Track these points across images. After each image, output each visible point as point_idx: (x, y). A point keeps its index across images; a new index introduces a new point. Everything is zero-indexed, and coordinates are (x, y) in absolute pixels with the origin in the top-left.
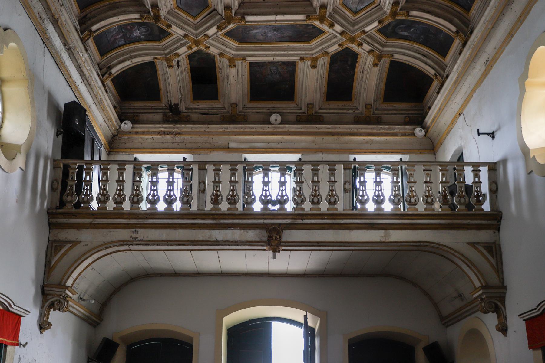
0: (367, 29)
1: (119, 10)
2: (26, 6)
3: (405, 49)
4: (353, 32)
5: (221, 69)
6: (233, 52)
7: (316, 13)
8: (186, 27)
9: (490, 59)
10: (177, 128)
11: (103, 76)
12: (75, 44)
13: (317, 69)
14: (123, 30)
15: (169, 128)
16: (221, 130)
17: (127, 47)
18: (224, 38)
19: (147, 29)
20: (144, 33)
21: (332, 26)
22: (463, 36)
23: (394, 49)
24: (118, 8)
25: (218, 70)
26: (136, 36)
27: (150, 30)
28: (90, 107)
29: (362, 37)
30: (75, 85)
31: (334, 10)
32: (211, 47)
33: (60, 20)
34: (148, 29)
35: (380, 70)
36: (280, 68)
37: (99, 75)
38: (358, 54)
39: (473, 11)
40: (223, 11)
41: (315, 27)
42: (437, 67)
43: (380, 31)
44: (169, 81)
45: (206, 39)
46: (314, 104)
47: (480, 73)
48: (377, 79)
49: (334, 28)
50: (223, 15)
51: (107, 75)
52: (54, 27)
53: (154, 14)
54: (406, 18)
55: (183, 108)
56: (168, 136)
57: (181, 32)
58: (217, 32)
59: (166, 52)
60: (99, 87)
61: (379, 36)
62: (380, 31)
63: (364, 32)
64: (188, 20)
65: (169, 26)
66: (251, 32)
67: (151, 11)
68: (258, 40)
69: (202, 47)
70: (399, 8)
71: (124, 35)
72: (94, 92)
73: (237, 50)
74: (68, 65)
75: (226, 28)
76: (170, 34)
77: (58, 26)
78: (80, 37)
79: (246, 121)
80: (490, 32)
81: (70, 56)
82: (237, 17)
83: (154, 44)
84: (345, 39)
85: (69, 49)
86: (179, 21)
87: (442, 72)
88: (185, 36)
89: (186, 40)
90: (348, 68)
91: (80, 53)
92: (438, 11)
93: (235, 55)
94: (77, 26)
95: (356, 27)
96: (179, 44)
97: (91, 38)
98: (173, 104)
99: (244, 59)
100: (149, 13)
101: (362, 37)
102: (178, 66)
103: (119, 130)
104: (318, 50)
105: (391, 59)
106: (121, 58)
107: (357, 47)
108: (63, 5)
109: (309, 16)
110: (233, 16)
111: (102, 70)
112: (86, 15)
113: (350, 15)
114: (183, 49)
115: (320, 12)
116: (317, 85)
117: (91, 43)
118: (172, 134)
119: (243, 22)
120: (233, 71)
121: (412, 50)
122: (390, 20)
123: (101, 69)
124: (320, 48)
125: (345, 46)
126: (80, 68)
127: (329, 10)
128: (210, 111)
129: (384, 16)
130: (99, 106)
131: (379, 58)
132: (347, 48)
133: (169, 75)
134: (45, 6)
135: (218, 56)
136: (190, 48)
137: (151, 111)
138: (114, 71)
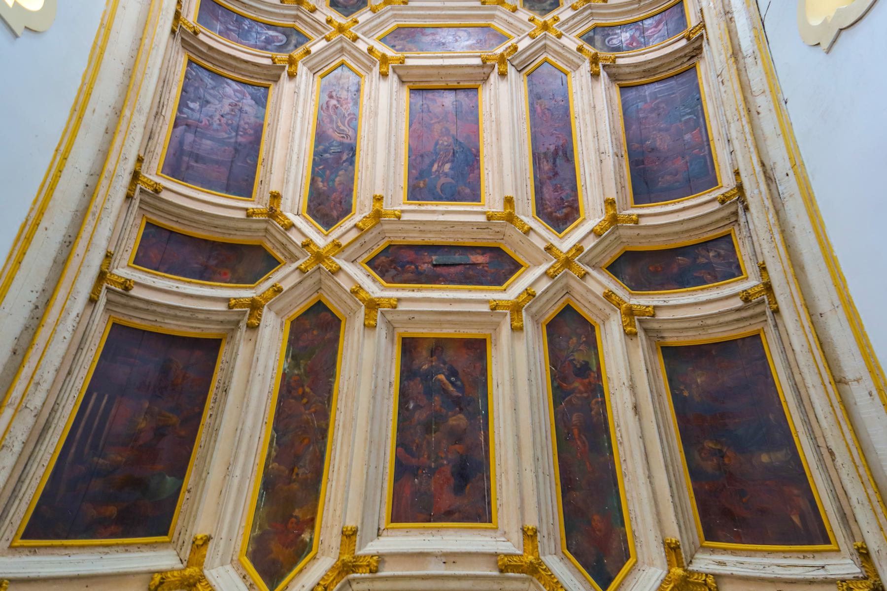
0: (324, 43)
1: (643, 68)
2: (772, 75)
3: (267, 11)
7: (392, 67)
8: (557, 48)
14: (643, 40)
17: (641, 15)
18: (510, 33)
20: (615, 36)
21: (371, 50)
24: (644, 71)
26: (626, 32)
29: (328, 33)
31: (371, 70)
34: (608, 42)
40: (509, 71)
41: (393, 47)
43: (307, 39)
53: (597, 64)
57: (564, 41)
61: (307, 31)
62: (307, 39)
63: (328, 39)
65: (580, 49)
66: (474, 42)
68: (465, 31)
70: (287, 68)
76: (580, 37)
83: (604, 22)
84: (351, 29)
86: (566, 56)
89: (560, 30)
92: (234, 63)
94: (707, 45)
95: (339, 46)
100: (604, 66)
101: (328, 33)
107: (333, 18)
115: (388, 69)
122: (297, 53)
124: (382, 18)
125: (350, 19)
127: (376, 70)
132: (347, 16)
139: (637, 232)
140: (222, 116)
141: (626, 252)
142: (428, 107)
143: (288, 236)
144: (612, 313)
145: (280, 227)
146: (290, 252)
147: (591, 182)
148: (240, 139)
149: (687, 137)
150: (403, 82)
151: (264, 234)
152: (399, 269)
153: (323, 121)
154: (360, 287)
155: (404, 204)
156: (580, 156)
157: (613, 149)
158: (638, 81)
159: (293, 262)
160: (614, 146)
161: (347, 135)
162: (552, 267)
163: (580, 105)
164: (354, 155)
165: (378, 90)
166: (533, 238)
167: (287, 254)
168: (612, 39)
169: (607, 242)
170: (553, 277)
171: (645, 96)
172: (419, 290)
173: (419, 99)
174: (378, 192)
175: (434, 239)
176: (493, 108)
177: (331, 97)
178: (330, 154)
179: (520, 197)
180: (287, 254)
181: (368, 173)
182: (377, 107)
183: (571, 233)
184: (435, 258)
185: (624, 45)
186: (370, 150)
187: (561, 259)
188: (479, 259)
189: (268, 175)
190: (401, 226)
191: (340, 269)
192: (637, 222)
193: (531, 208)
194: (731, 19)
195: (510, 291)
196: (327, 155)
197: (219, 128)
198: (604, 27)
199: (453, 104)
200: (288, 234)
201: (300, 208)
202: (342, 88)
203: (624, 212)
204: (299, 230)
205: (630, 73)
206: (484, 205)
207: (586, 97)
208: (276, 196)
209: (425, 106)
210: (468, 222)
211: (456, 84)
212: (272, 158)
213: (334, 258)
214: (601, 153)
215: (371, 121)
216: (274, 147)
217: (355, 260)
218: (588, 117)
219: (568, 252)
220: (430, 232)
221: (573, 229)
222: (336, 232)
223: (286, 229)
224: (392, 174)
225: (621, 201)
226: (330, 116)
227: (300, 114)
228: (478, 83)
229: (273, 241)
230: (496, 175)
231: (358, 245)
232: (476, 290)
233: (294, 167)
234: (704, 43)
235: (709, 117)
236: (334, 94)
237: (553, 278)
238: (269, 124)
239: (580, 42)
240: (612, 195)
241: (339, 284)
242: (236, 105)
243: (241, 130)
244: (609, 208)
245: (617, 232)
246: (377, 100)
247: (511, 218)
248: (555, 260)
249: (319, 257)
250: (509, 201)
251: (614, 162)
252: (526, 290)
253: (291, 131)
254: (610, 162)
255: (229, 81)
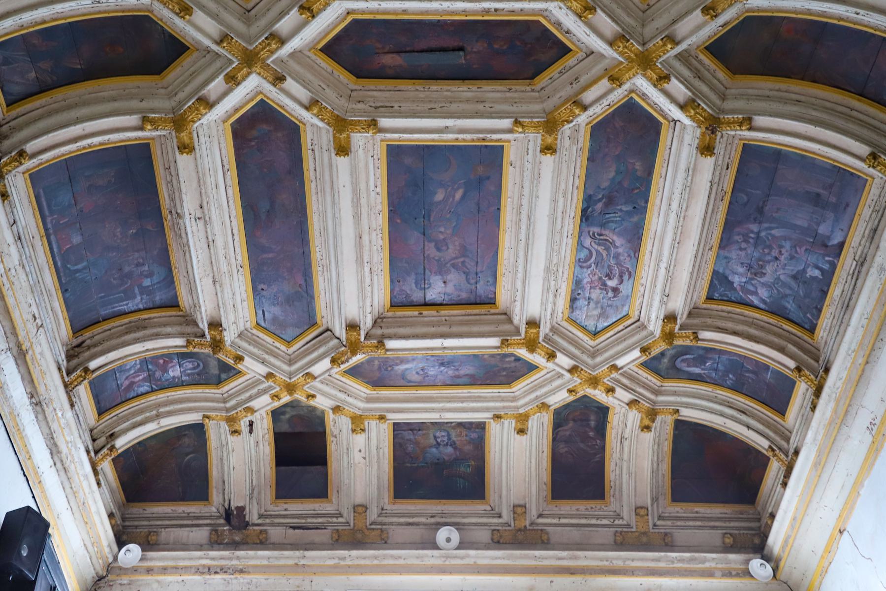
0: (620, 363)
4: (594, 367)
5: (335, 437)
6: (362, 405)
7: (520, 335)
8: (272, 360)
9: (877, 422)
10: (238, 558)
11: (96, 452)
12: (53, 394)
13: (528, 437)
14: (150, 367)
15: (221, 559)
16: (331, 562)
18: (343, 379)
19: (196, 364)
20: (189, 372)
21: (551, 356)
22: (812, 377)
23: (679, 399)
24: (145, 328)
25: (329, 438)
26: (174, 377)
27: (201, 365)
28: (60, 516)
29: (612, 376)
30: (36, 473)
31: (553, 329)
32: (318, 396)
33: (30, 352)
34: (198, 365)
35: (657, 439)
36: (453, 434)
37: (88, 452)
38: (607, 408)
39: (821, 333)
41: (518, 359)
42: (771, 434)
43: (645, 365)
44: (229, 461)
45: (309, 380)
46: (527, 506)
47: (864, 450)
48: (653, 455)
49: (557, 360)
50: (344, 338)
51: (105, 451)
52: (17, 364)
53: (214, 339)
54: (694, 343)
55: (253, 516)
56: (218, 577)
57: (263, 370)
58: (331, 368)
59: (228, 405)
60: (86, 477)
62: (645, 365)
63: (614, 368)
64: (276, 347)
65: (240, 359)
66: (396, 368)
67: (207, 333)
68: (410, 381)
69: (300, 396)
70: (677, 327)
71: (149, 375)
72: (73, 486)
73: (369, 400)
74: (29, 435)
75: (347, 361)
76: (239, 373)
77: (26, 362)
78: (64, 382)
79: (386, 542)
80: (863, 371)
81: (36, 417)
82: (369, 342)
84: (579, 381)
85: (37, 403)
86: (259, 349)
87: (784, 444)
88: (269, 376)
89: (270, 383)
90: (591, 434)
91: (58, 411)
93: (364, 410)
95: (599, 359)
96: (254, 391)
97: (86, 382)
98: (233, 508)
99: (382, 418)
100: (203, 336)
101: (612, 376)
102: (251, 432)
103: (114, 565)
104: (527, 399)
105: (676, 416)
106: (139, 418)
107: (604, 395)
108: (42, 326)
109: (507, 340)
110: (362, 339)
111: (97, 442)
112: (83, 342)
113: (585, 338)
114: (265, 399)
115: (526, 332)
116: (530, 468)
117: (83, 392)
118: (225, 572)
119: (380, 353)
120: (360, 439)
121: (715, 400)
122: (662, 346)
123: (94, 440)
124: (533, 396)
125: (581, 393)
126: (53, 438)
127: (544, 329)
128: (309, 520)
129: (650, 339)
130: (77, 515)
131: (652, 414)
132: (585, 396)
133: (230, 449)
134: (7, 329)
135: (331, 412)
136: (276, 397)
137: (185, 522)
138: (122, 443)
139: (144, 105)
140: (776, 259)
141: (159, 73)
142: (468, 280)
143: (690, 90)
145: (703, 105)
146: (689, 66)
147: (216, 176)
148: (755, 227)
149: (77, 239)
150: (505, 314)
151: (728, 91)
152: (518, 43)
153: (629, 256)
154: (580, 17)
155: (509, 141)
156: (233, 213)
157: (185, 224)
158: (152, 315)
159: (685, 50)
160: (182, 228)
161: (593, 237)
162: (272, 52)
163: (236, 284)
164: (584, 211)
165: (542, 303)
166: (303, 94)
167: (694, 62)
168: (194, 368)
169: (188, 89)
170: (273, 36)
171: (141, 294)
172: (487, 11)
173: (482, 289)
174: (548, 159)
175: (461, 89)
176: (368, 281)
177: (615, 290)
178: (621, 210)
179: (326, 155)
180: (694, 62)
181: (563, 186)
182: (546, 280)
183: (244, 101)
184: (459, 59)
185: (176, 361)
186: (559, 219)
187: (259, 65)
188: (389, 60)
189: (717, 179)
190: (514, 109)
191: (611, 44)
192: (145, 119)
193: (307, 137)
194: (32, 397)
195: (340, 12)
196: (624, 208)
197: (783, 243)
198: (207, 383)
199: (430, 284)
200: (690, 94)
201: (671, 131)
202: (597, 303)
203: (163, 133)
204: (673, 99)
205: (165, 325)
206: (382, 140)
207: (228, 294)
208: (707, 149)
209: (472, 281)
210: (406, 117)
211: (425, 313)
212: (708, 204)
213: (621, 59)
214: (203, 218)
215: (555, 261)
216: (705, 219)
217: (588, 56)
218: (224, 268)
219: (249, 74)
220: (468, 101)
221: (241, 108)
222: (618, 96)
223: (694, 101)
224: (527, 185)
225: (170, 149)
226: (619, 264)
227: (663, 265)
228: (390, 314)
229: (715, 81)
230: (363, 186)
231: (583, 80)
232: (395, 12)
233: (677, 192)
234: (64, 364)
235: (49, 268)
236: (611, 294)
237: (271, 34)
238: (710, 249)
239: (240, 366)
240: (183, 161)
241: (614, 20)
242: (755, 275)
243: (751, 241)
244: (186, 140)
245: (174, 104)
246: (546, 289)
247: (340, 124)
248: (269, 62)
249: (645, 62)
250: (343, 150)
251: (182, 206)
252: (313, 17)
253: (677, 243)
254: (189, 204)
255: (762, 306)
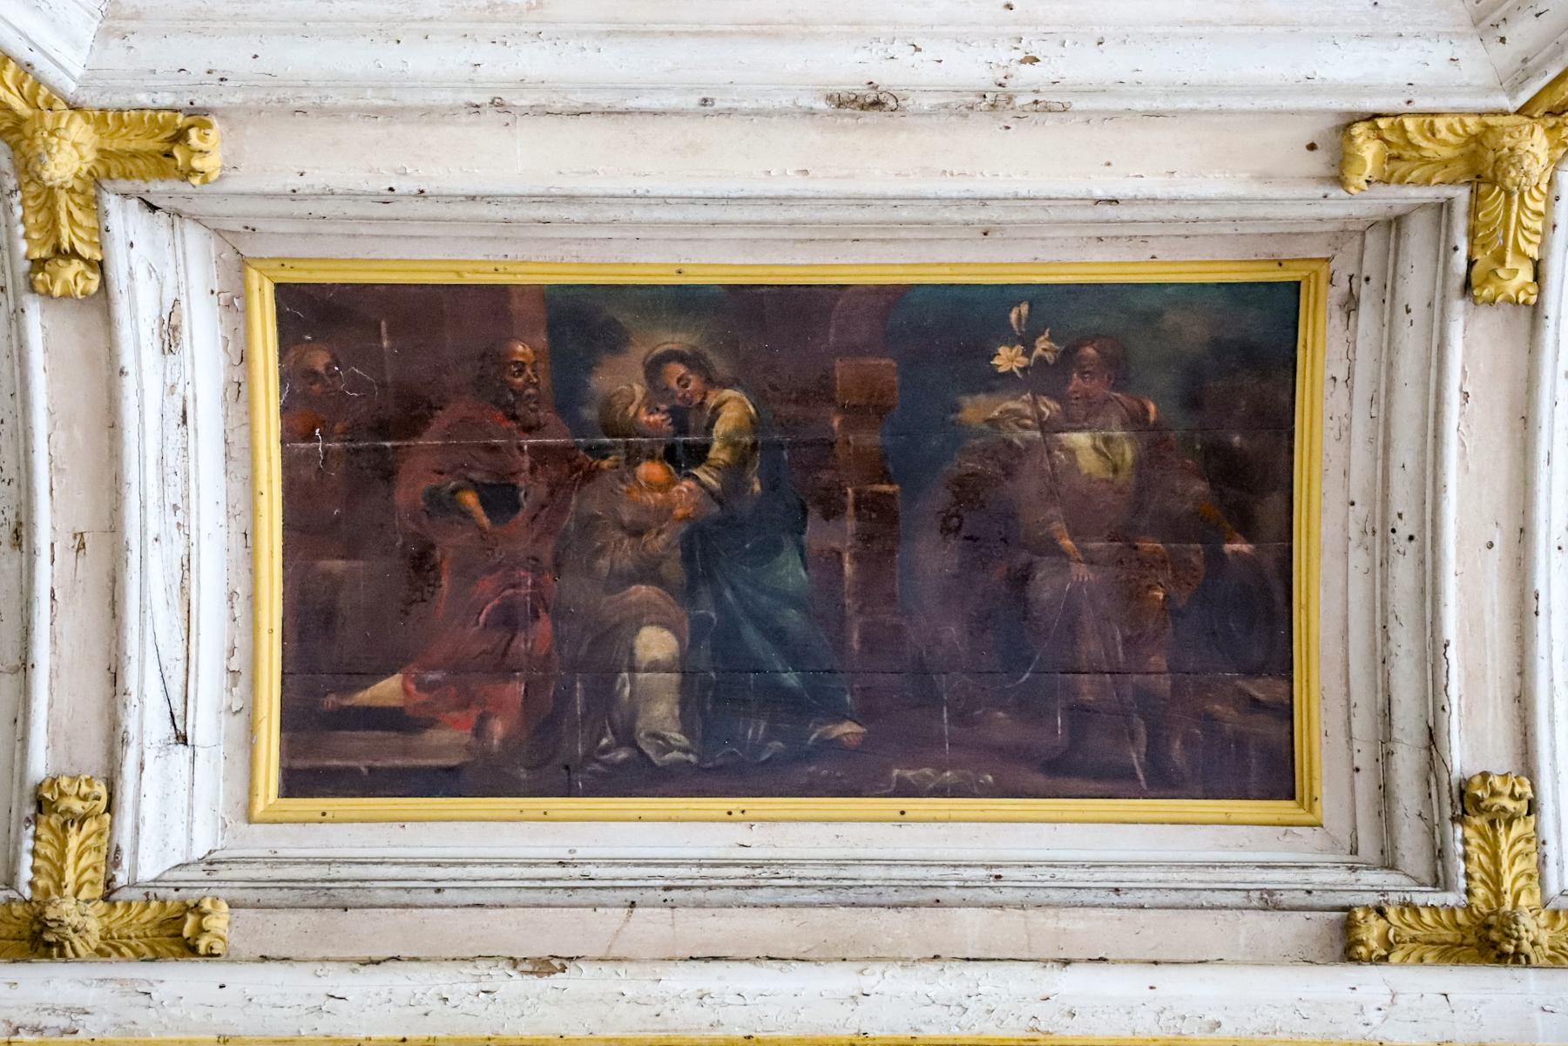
144: (1506, 56)
